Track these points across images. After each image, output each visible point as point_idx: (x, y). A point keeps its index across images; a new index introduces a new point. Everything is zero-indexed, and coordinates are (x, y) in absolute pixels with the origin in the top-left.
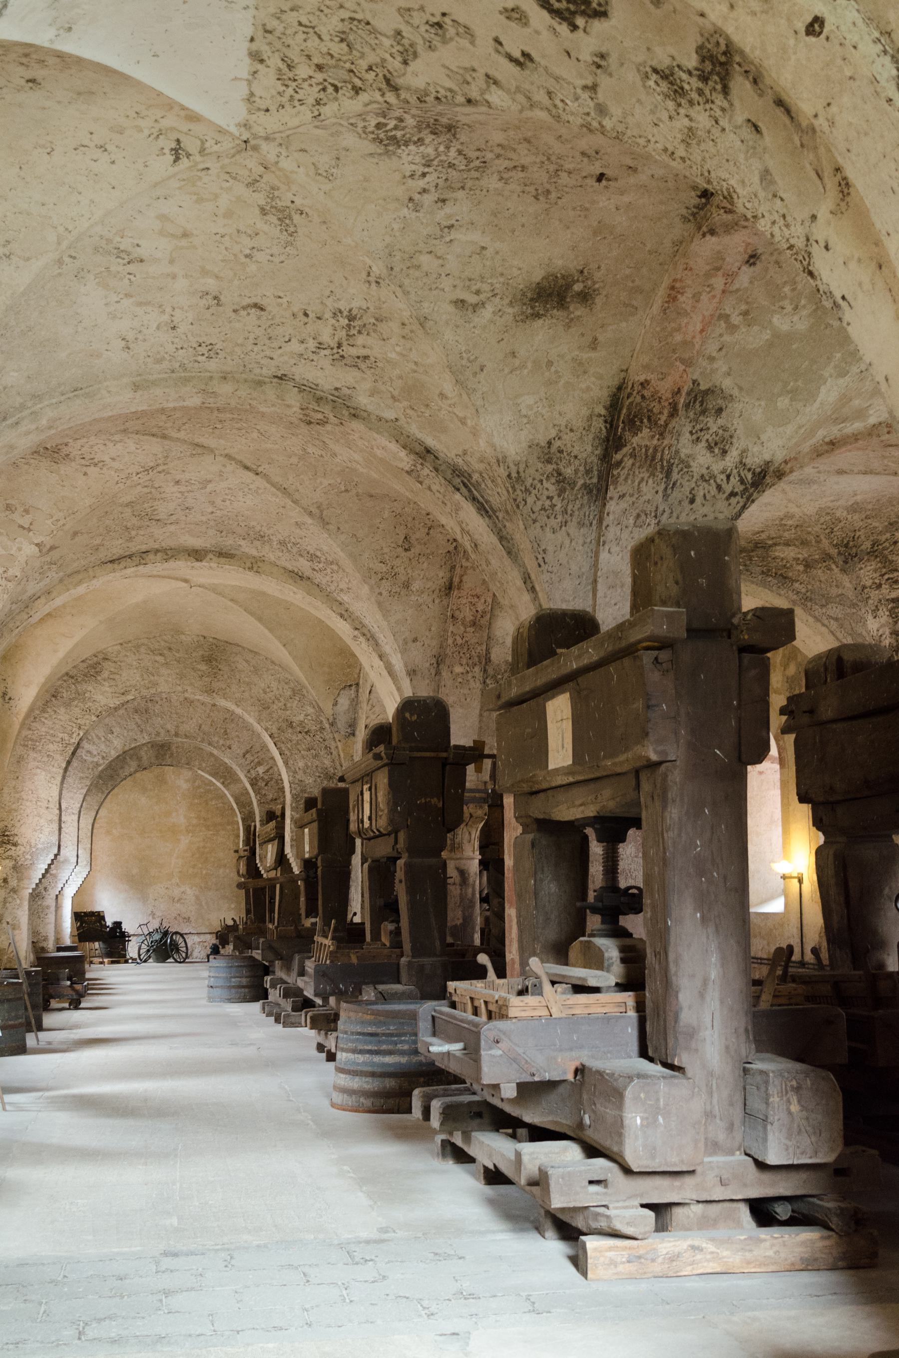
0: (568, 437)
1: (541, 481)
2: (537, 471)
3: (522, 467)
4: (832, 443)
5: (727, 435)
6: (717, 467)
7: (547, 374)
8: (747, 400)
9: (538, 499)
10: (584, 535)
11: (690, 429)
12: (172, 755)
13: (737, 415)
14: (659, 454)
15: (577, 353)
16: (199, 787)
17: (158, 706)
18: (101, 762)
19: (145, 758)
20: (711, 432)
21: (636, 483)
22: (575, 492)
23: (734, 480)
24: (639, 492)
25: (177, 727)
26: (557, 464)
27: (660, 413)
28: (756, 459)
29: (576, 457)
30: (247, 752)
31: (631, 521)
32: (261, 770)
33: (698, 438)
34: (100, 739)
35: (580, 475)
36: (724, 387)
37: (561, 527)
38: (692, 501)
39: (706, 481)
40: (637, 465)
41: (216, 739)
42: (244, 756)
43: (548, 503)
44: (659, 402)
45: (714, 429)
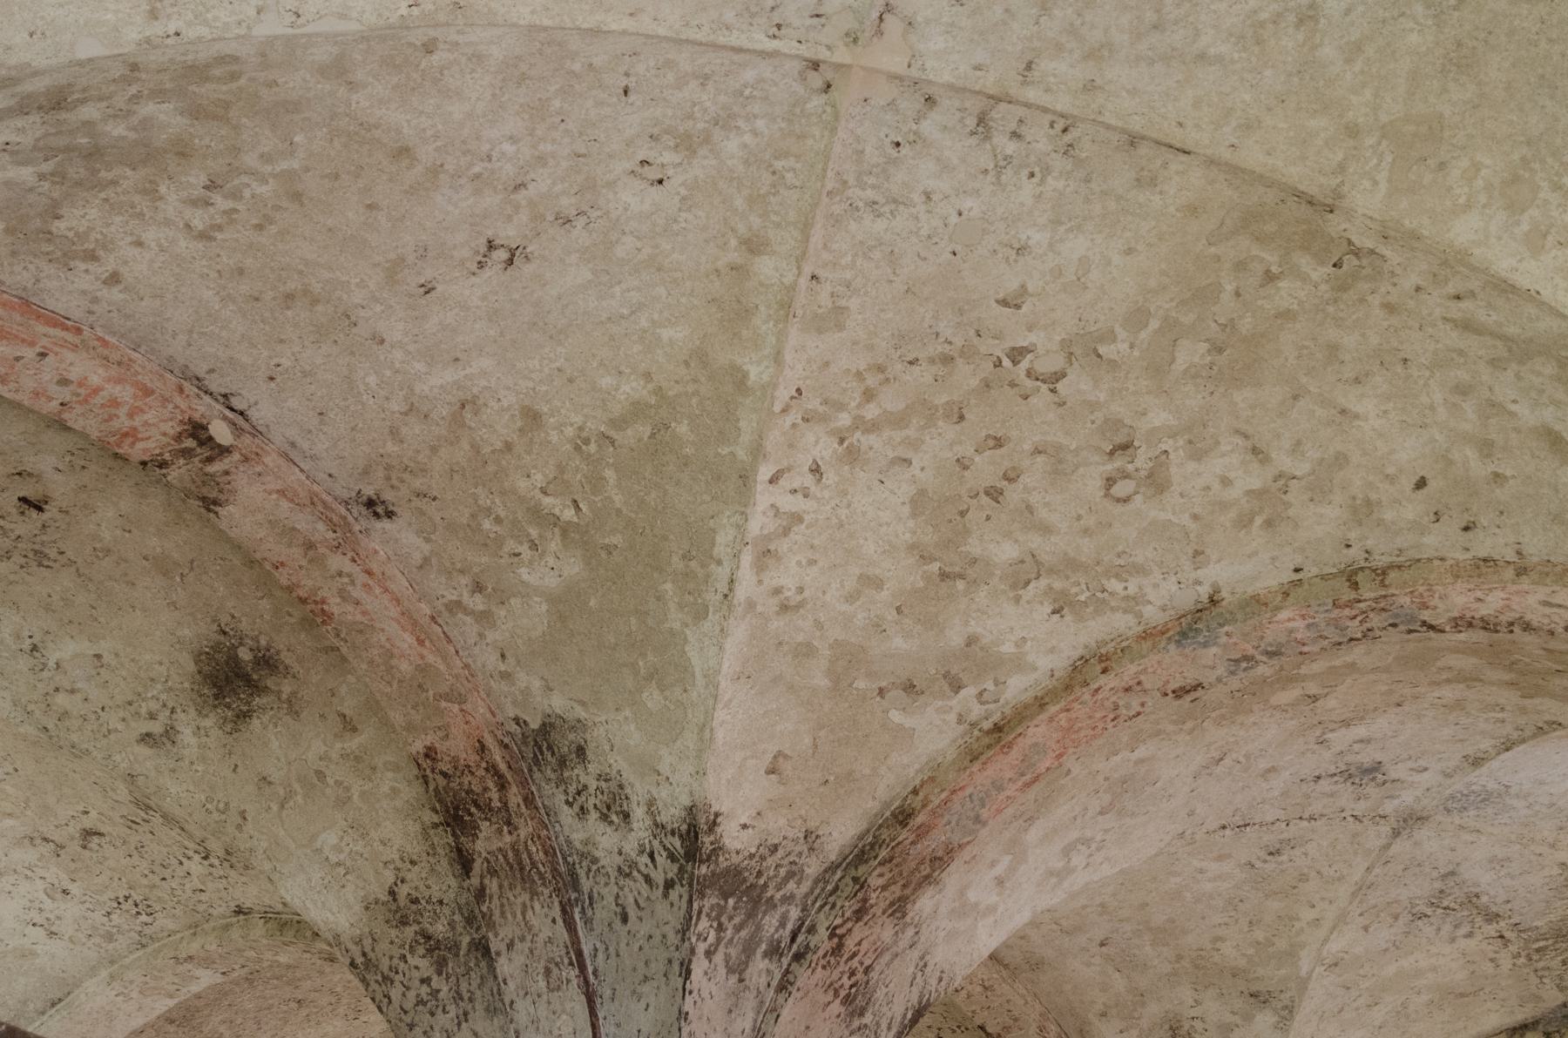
0: (413, 875)
1: (403, 958)
2: (392, 943)
3: (367, 942)
4: (998, 728)
5: (613, 785)
6: (630, 847)
7: (328, 791)
8: (603, 718)
9: (408, 988)
10: (502, 1028)
11: (563, 798)
13: (607, 748)
14: (525, 856)
15: (338, 745)
20: (592, 790)
21: (519, 916)
22: (462, 960)
23: (661, 859)
24: (530, 930)
26: (419, 923)
27: (486, 789)
28: (673, 810)
29: (441, 902)
31: (542, 984)
33: (582, 808)
35: (459, 929)
36: (558, 711)
37: (459, 1024)
38: (625, 919)
39: (628, 875)
40: (506, 884)
43: (425, 989)
44: (473, 774)
45: (593, 784)
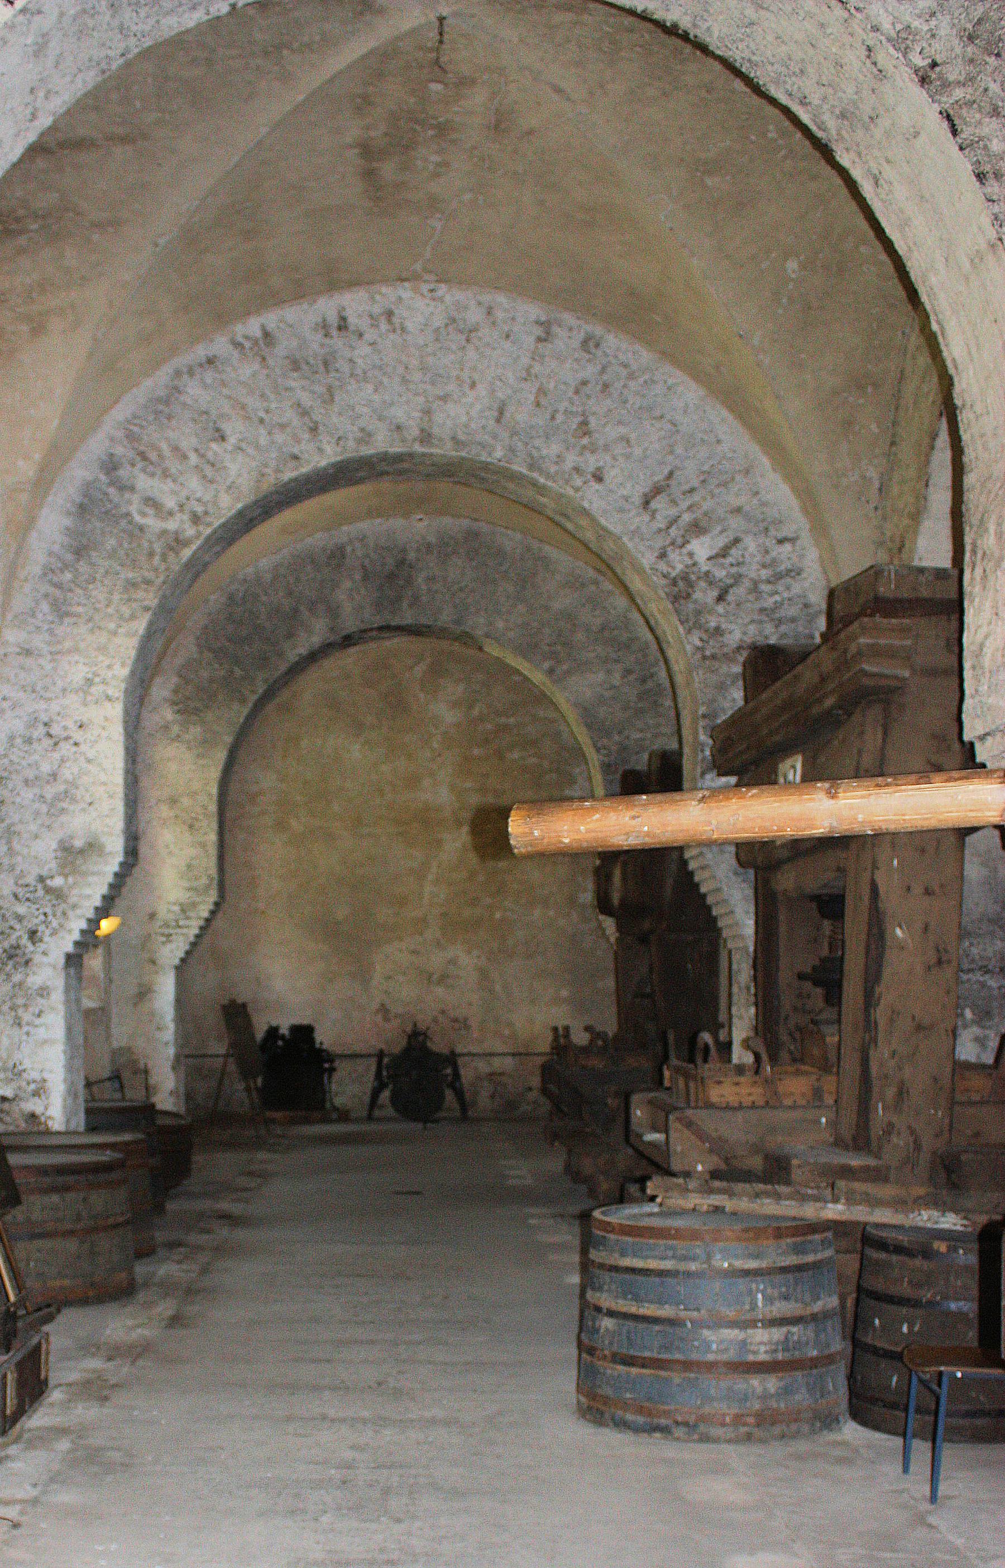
12: (415, 601)
16: (481, 719)
17: (362, 350)
18: (190, 531)
19: (347, 608)
25: (427, 412)
30: (657, 490)
32: (701, 548)
34: (185, 457)
41: (554, 448)
42: (646, 503)
